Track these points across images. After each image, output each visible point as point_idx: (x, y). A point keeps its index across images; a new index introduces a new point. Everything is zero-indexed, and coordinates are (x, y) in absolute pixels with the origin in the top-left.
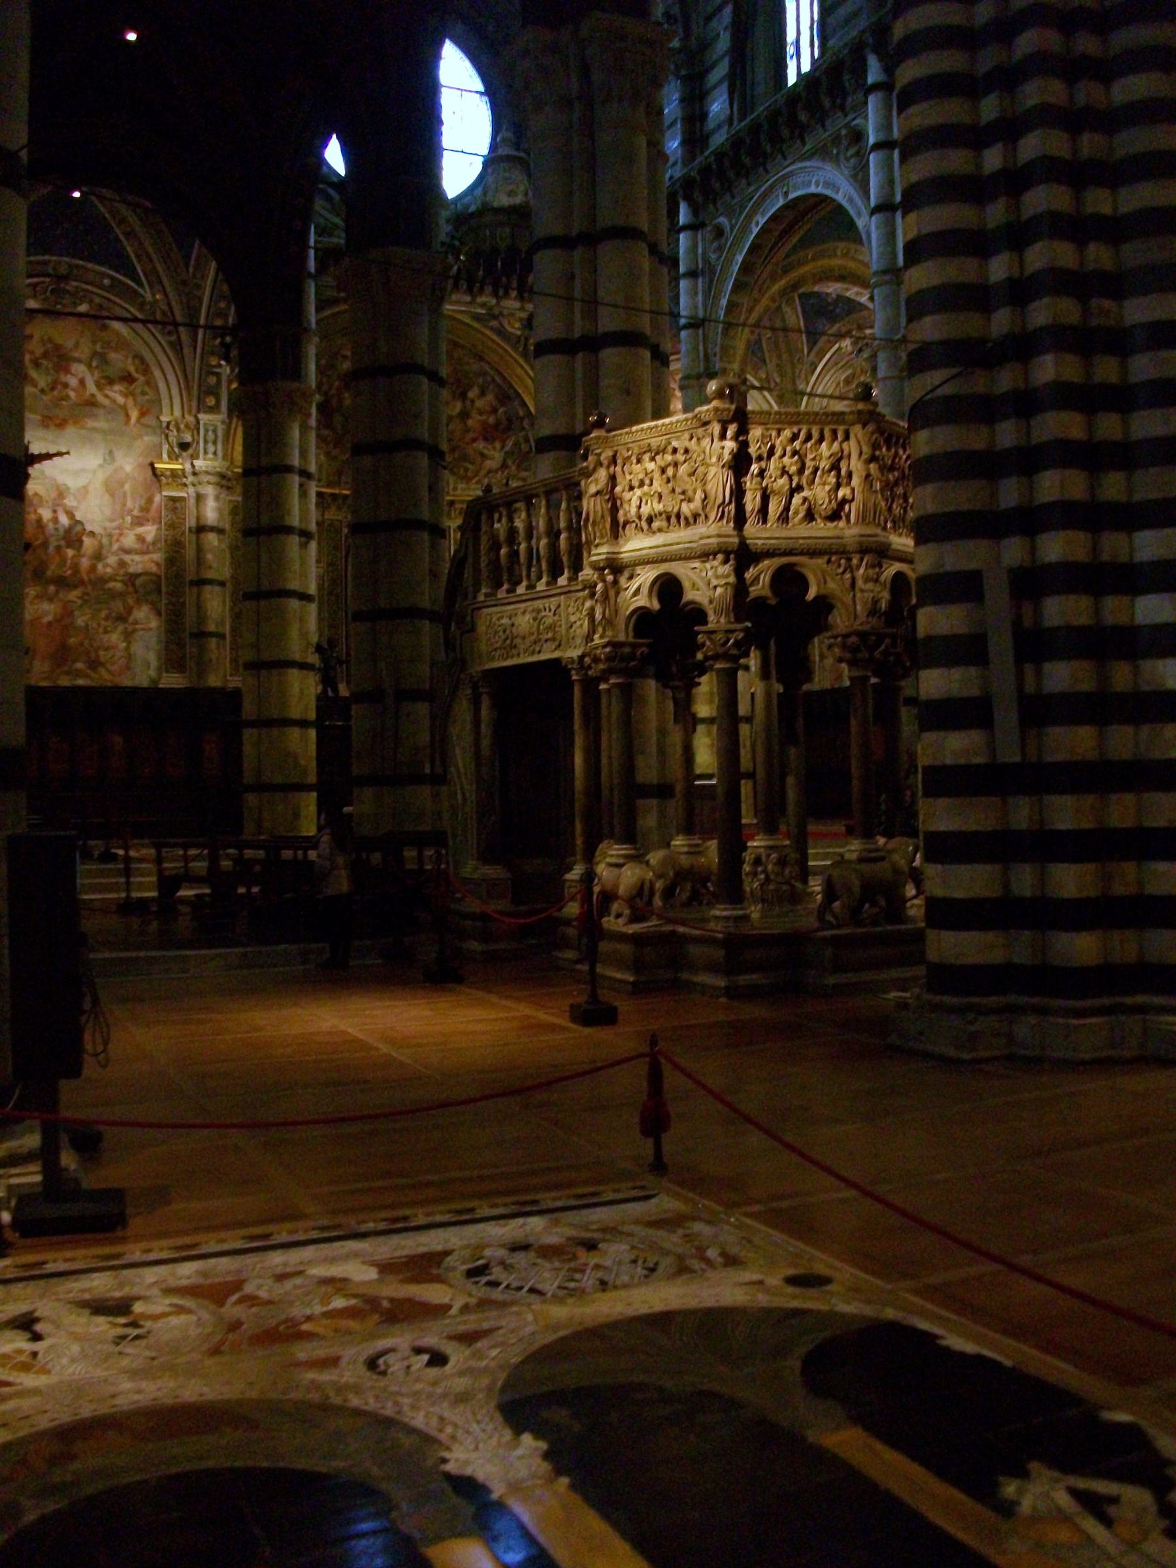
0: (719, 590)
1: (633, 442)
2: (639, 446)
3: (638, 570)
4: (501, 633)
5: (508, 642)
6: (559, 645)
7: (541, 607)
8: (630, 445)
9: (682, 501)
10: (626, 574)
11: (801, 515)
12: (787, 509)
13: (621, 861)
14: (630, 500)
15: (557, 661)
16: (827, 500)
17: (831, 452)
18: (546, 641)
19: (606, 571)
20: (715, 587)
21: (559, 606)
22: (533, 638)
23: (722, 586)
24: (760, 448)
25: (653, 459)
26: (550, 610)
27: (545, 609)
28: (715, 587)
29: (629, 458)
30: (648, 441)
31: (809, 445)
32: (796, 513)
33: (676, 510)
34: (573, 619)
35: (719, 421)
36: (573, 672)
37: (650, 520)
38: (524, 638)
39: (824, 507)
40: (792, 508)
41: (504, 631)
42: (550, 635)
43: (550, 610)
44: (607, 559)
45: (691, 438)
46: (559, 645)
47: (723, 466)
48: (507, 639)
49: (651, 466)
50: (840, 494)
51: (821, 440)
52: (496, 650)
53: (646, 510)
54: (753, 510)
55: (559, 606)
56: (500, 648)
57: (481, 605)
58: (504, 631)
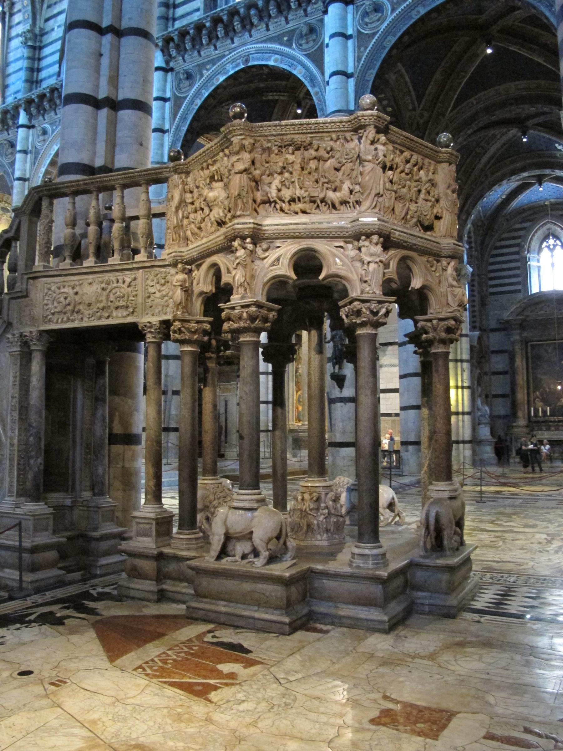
0: (372, 266)
1: (274, 136)
2: (282, 140)
3: (278, 243)
4: (62, 299)
5: (69, 308)
6: (133, 313)
7: (114, 279)
8: (270, 138)
9: (327, 189)
10: (265, 246)
11: (414, 220)
12: (407, 213)
13: (255, 505)
14: (270, 183)
15: (134, 326)
16: (430, 213)
17: (429, 178)
18: (117, 308)
19: (248, 240)
20: (369, 263)
21: (135, 279)
22: (101, 305)
23: (376, 262)
24: (393, 160)
25: (293, 153)
26: (124, 282)
27: (118, 282)
28: (369, 263)
29: (269, 149)
30: (293, 136)
31: (415, 169)
32: (412, 217)
33: (322, 196)
34: (151, 290)
35: (376, 127)
36: (148, 335)
37: (292, 200)
38: (90, 305)
39: (428, 217)
40: (410, 213)
41: (66, 298)
42: (122, 303)
43: (124, 282)
44: (254, 228)
45: (338, 139)
46: (133, 313)
47: (379, 163)
48: (69, 305)
49: (291, 158)
50: (435, 211)
51: (421, 168)
52: (53, 314)
53: (287, 194)
54: (389, 208)
55: (135, 279)
56: (59, 313)
57: (43, 274)
58: (66, 298)
